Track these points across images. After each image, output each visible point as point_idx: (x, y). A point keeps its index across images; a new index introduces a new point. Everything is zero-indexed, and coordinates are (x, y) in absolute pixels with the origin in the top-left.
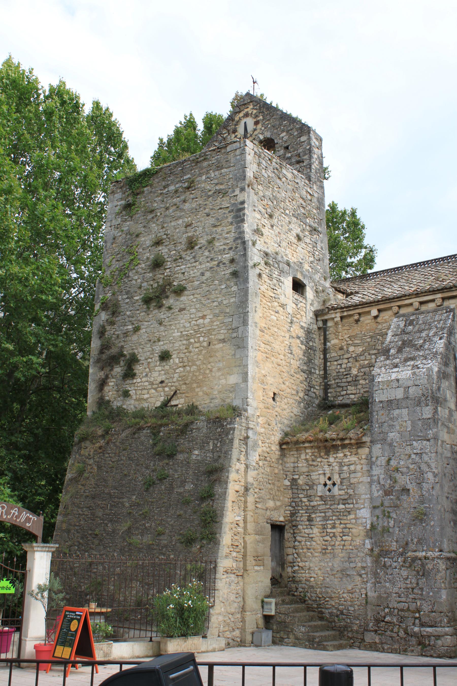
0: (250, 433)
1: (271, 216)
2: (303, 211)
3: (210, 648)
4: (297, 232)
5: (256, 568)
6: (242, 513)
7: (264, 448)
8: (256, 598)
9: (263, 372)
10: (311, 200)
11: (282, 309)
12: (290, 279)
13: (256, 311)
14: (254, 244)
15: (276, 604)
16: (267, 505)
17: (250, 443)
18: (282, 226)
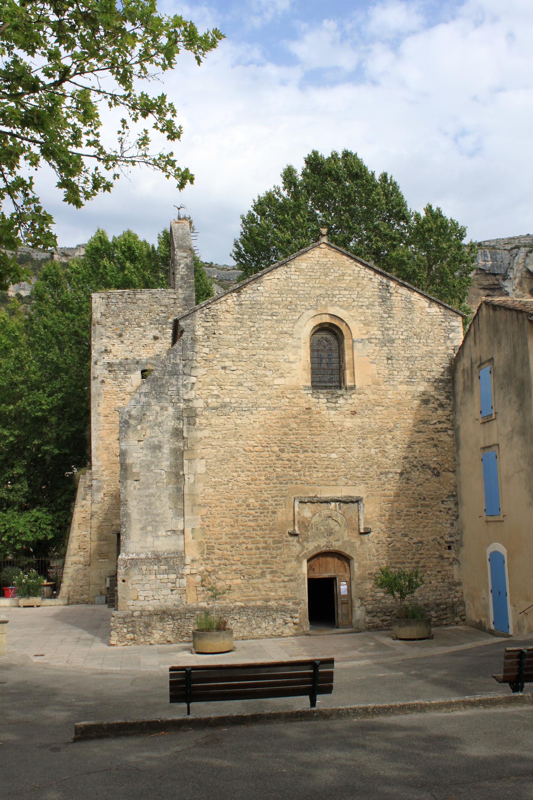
0: (94, 483)
1: (121, 335)
2: (165, 315)
3: (58, 604)
4: (154, 334)
5: (100, 560)
6: (89, 529)
7: (110, 489)
8: (101, 577)
9: (108, 442)
10: (175, 303)
11: (129, 396)
12: (139, 372)
13: (98, 406)
14: (96, 363)
15: (110, 581)
16: (114, 523)
17: (94, 487)
18: (134, 337)
